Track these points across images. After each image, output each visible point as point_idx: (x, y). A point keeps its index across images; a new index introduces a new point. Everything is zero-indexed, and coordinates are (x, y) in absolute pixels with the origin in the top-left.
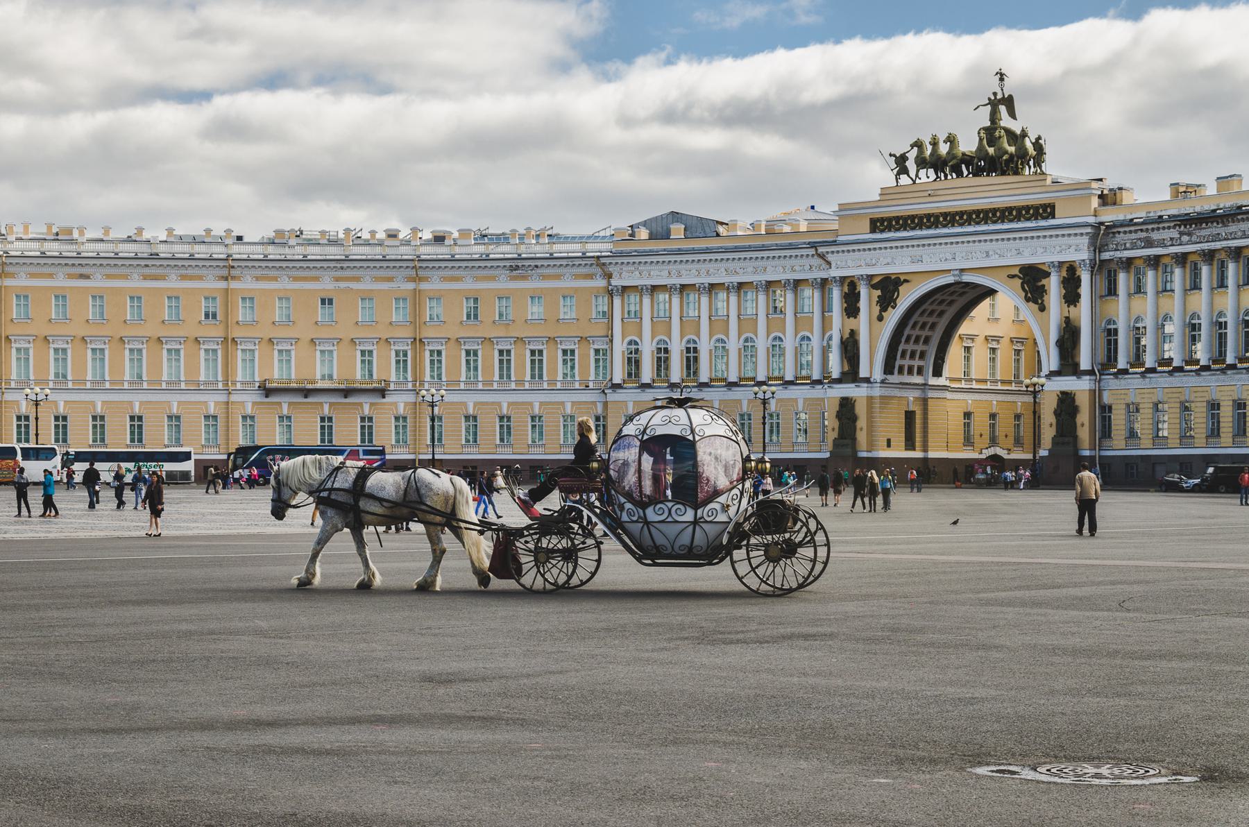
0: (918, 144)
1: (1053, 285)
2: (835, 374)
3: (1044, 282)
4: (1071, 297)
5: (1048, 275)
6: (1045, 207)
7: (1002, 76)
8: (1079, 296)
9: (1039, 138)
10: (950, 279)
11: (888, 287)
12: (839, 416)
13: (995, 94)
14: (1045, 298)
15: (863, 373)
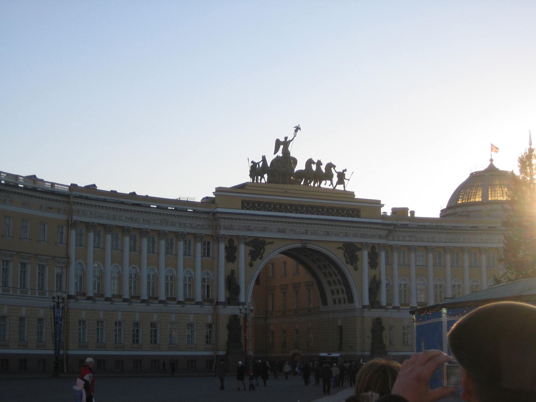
0: (264, 158)
1: (364, 256)
2: (222, 298)
3: (357, 253)
4: (373, 263)
5: (360, 249)
6: (353, 210)
7: (297, 129)
8: (377, 264)
9: (345, 170)
10: (299, 245)
11: (257, 247)
12: (230, 327)
13: (286, 138)
14: (358, 263)
15: (242, 299)
